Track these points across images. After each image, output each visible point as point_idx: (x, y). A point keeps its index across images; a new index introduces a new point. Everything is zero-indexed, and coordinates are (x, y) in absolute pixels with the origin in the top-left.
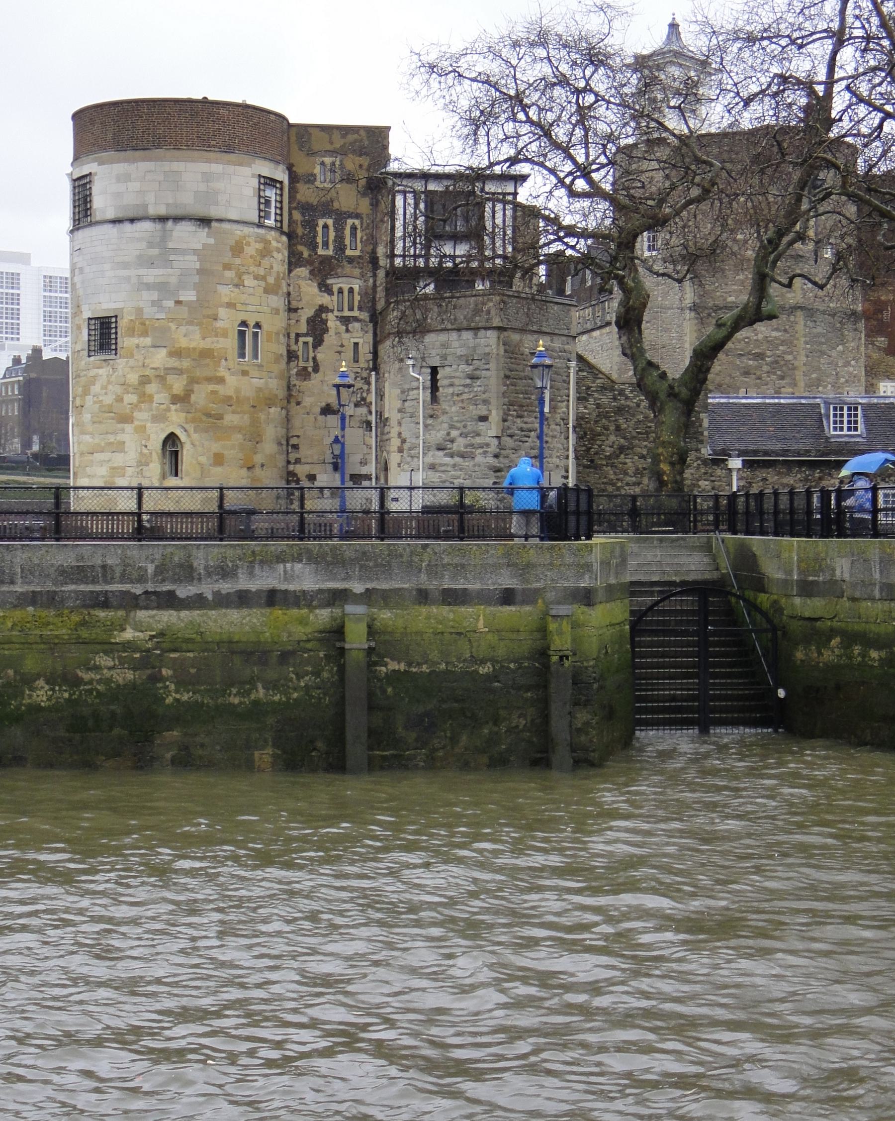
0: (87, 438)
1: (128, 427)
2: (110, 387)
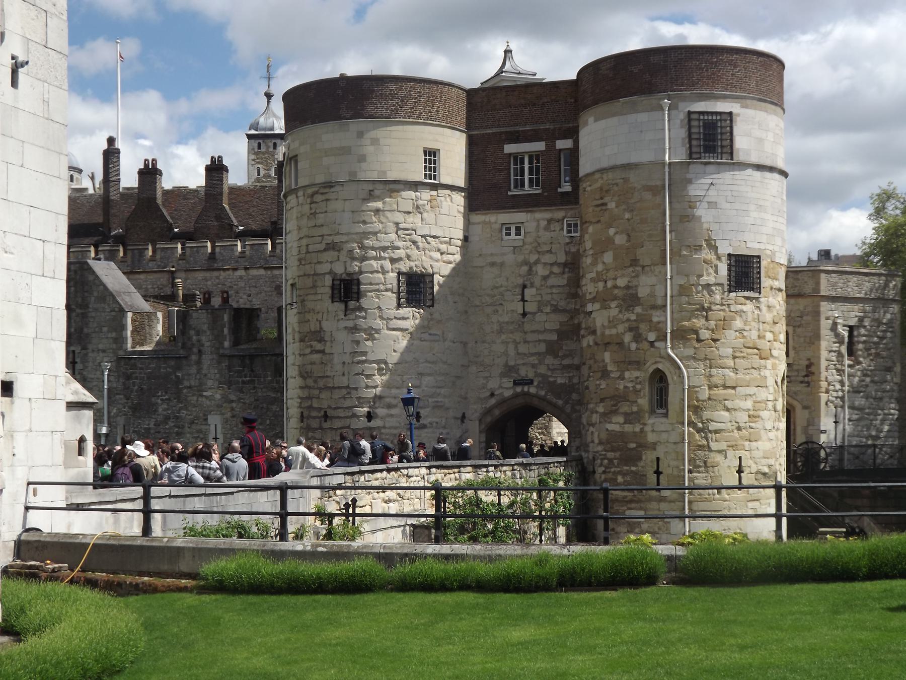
1: (769, 363)
2: (753, 324)
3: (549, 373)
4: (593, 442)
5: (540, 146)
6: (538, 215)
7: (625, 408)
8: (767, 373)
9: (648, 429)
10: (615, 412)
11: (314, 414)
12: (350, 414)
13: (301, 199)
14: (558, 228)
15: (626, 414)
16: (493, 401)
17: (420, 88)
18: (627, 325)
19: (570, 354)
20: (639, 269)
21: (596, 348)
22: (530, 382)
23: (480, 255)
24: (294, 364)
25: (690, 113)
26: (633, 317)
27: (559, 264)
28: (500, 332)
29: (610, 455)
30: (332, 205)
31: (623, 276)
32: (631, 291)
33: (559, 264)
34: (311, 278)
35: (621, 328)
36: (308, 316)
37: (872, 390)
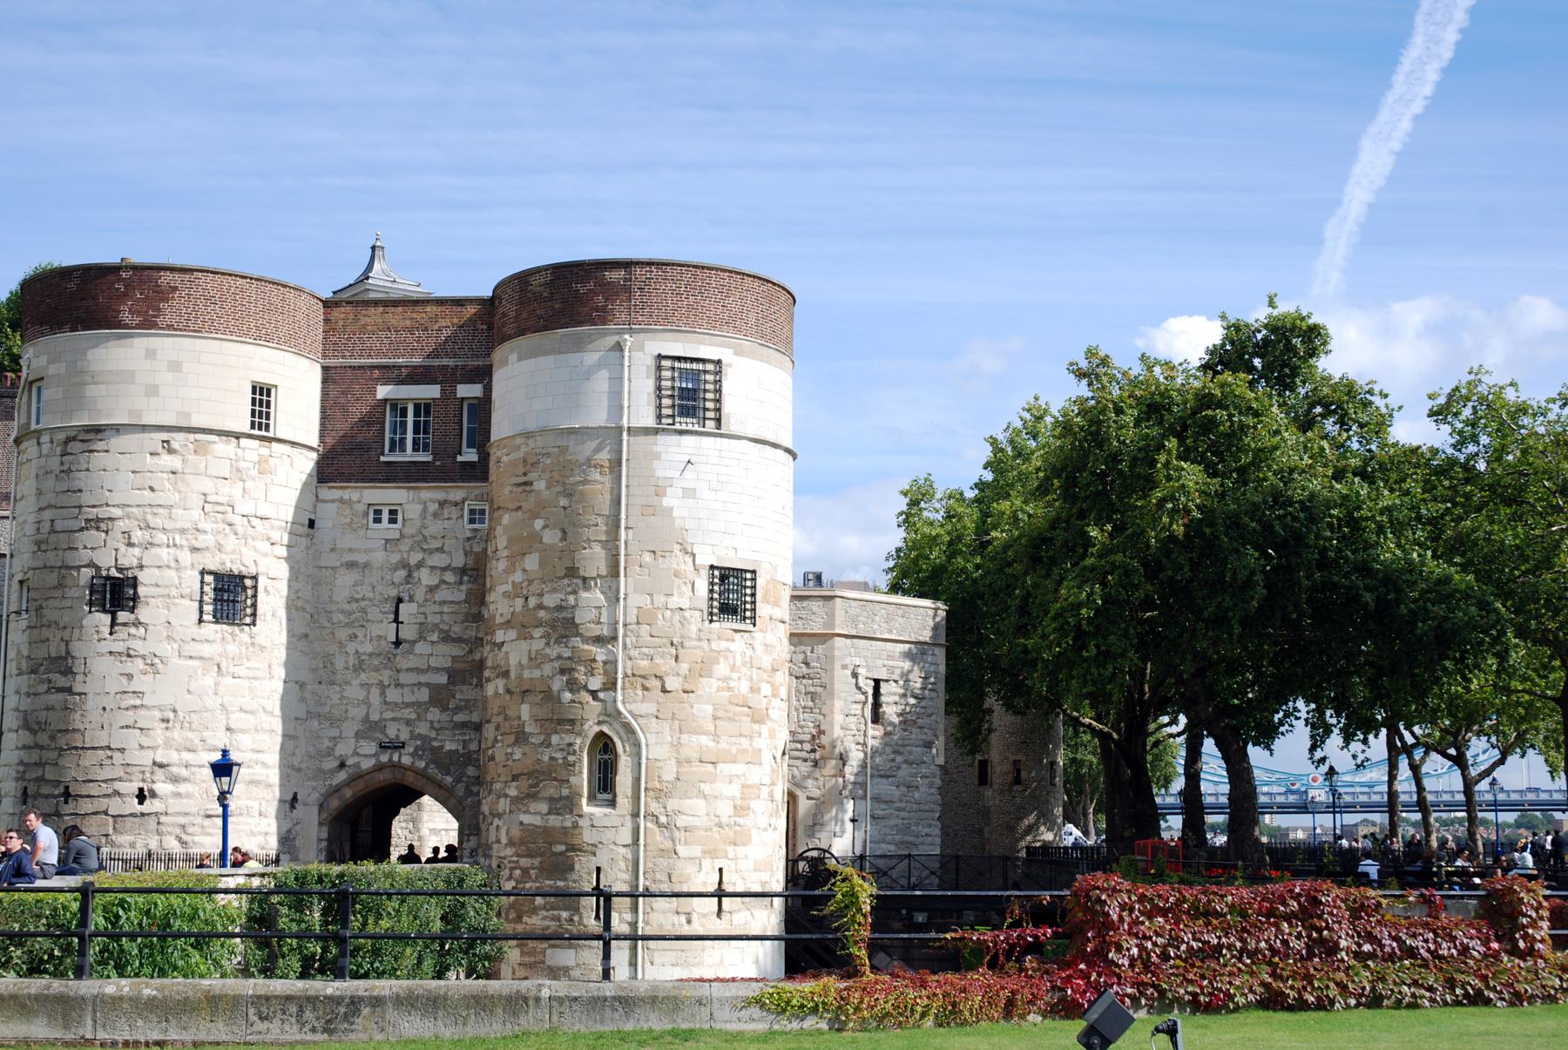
0: (705, 741)
1: (765, 729)
2: (744, 670)
3: (433, 735)
4: (498, 841)
5: (432, 391)
6: (426, 495)
7: (550, 790)
8: (759, 743)
9: (583, 823)
10: (533, 796)
11: (45, 790)
12: (110, 791)
13: (46, 448)
14: (454, 516)
15: (551, 800)
16: (342, 776)
17: (275, 294)
18: (556, 664)
19: (468, 706)
20: (580, 582)
21: (508, 697)
22: (401, 746)
23: (332, 550)
24: (16, 709)
25: (660, 357)
26: (567, 653)
27: (454, 570)
28: (359, 668)
29: (525, 862)
30: (98, 460)
31: (554, 590)
32: (564, 615)
33: (454, 570)
34: (55, 574)
35: (547, 669)
36: (46, 633)
37: (904, 772)
